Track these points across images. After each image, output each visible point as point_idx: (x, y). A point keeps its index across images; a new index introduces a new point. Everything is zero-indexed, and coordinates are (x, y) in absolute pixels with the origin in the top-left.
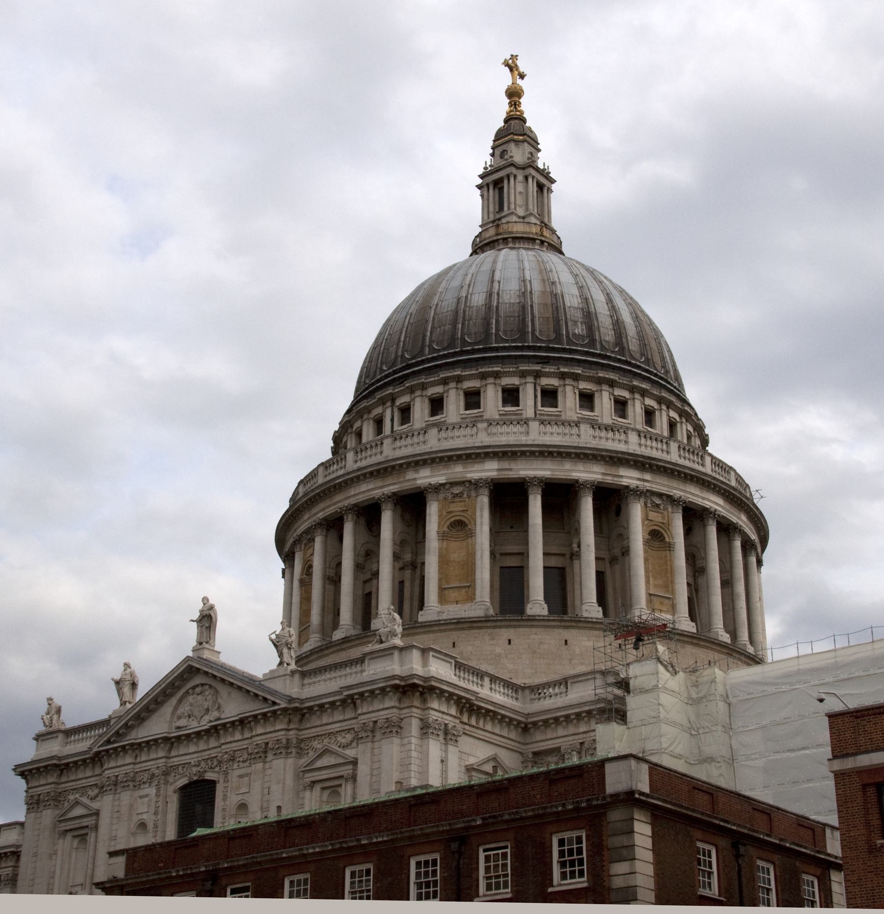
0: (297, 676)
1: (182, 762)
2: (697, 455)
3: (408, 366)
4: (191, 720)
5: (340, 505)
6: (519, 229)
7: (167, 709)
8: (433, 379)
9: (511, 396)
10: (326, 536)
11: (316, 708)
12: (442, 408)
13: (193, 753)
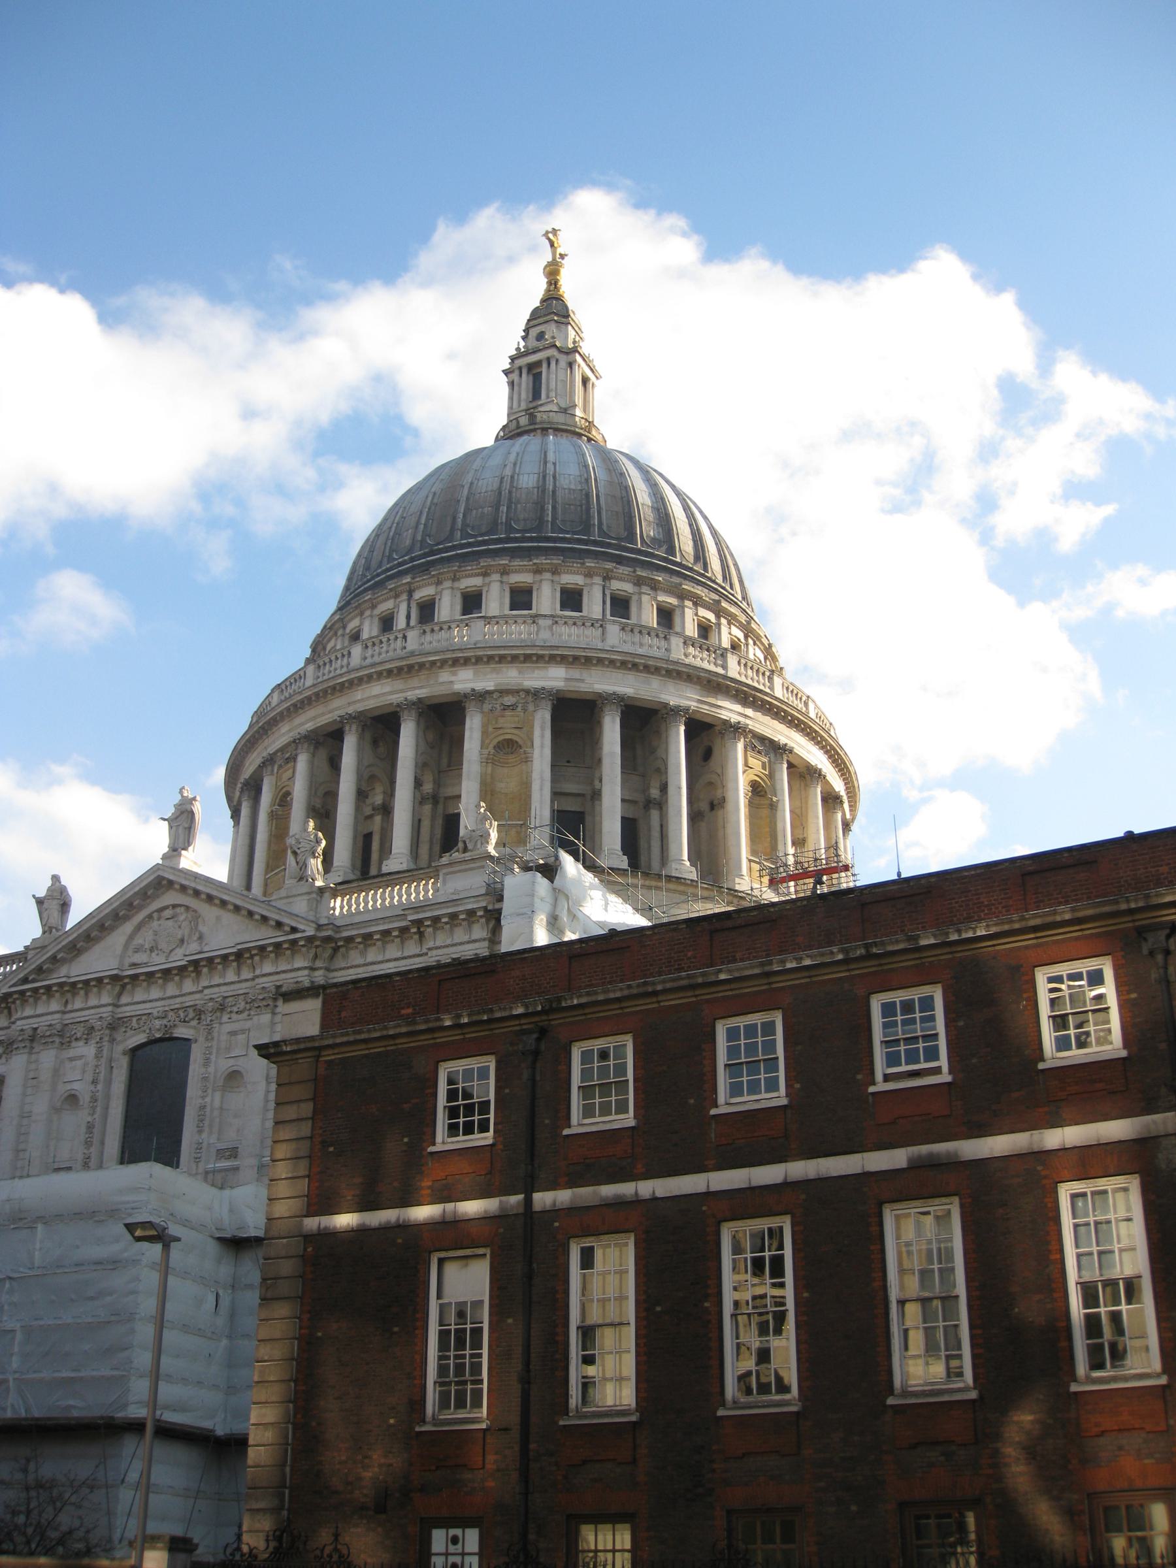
1: (138, 1013)
2: (801, 699)
3: (432, 553)
5: (342, 712)
6: (560, 418)
7: (118, 938)
10: (314, 755)
13: (156, 1000)
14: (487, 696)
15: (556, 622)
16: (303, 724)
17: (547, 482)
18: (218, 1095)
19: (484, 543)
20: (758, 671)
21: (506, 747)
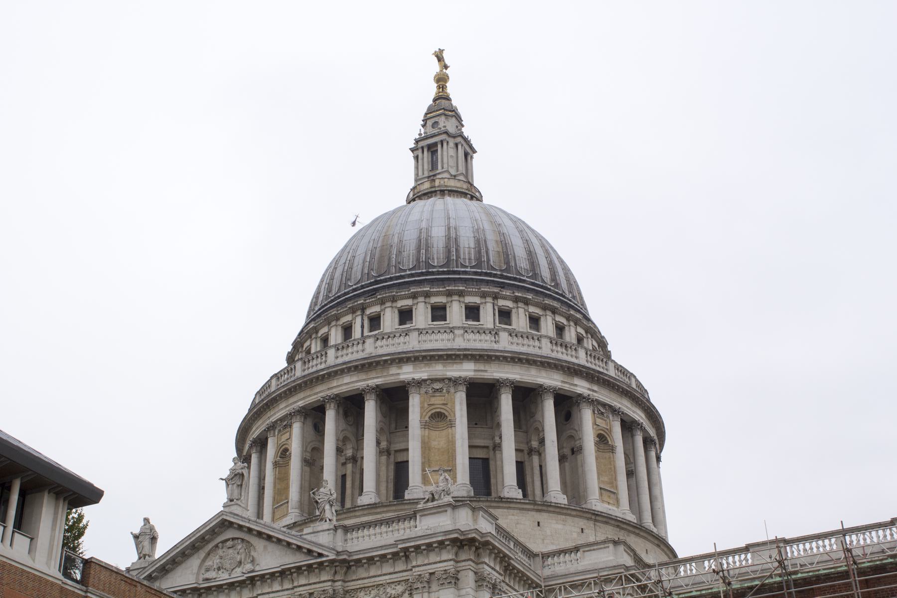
0: (340, 531)
2: (626, 375)
3: (376, 282)
4: (220, 572)
6: (452, 184)
7: (194, 562)
8: (404, 293)
9: (473, 312)
11: (365, 561)
12: (412, 320)
14: (423, 383)
15: (466, 331)
17: (451, 232)
19: (412, 275)
20: (594, 357)
21: (437, 417)
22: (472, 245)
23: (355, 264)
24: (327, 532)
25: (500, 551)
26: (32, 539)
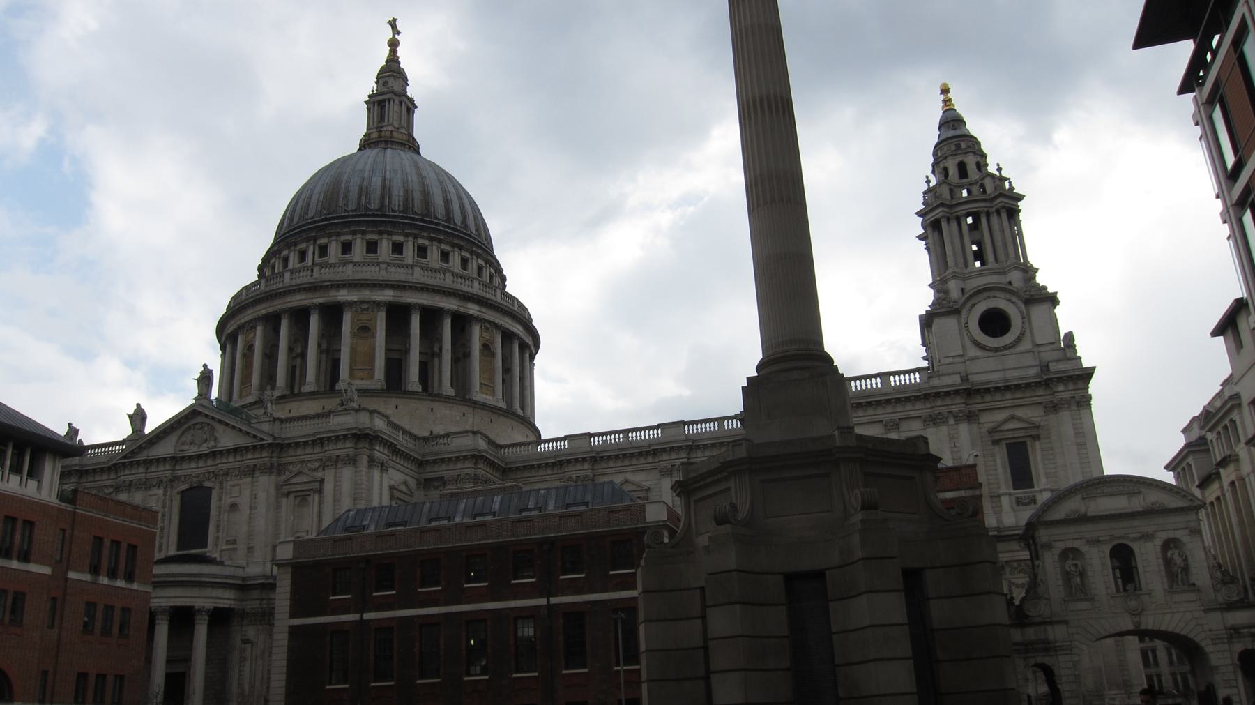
3: (326, 219)
4: (192, 446)
5: (279, 307)
7: (173, 438)
9: (398, 248)
11: (293, 445)
12: (351, 250)
16: (260, 310)
18: (226, 514)
22: (402, 194)
23: (312, 201)
24: (268, 423)
25: (387, 441)
26: (39, 482)
